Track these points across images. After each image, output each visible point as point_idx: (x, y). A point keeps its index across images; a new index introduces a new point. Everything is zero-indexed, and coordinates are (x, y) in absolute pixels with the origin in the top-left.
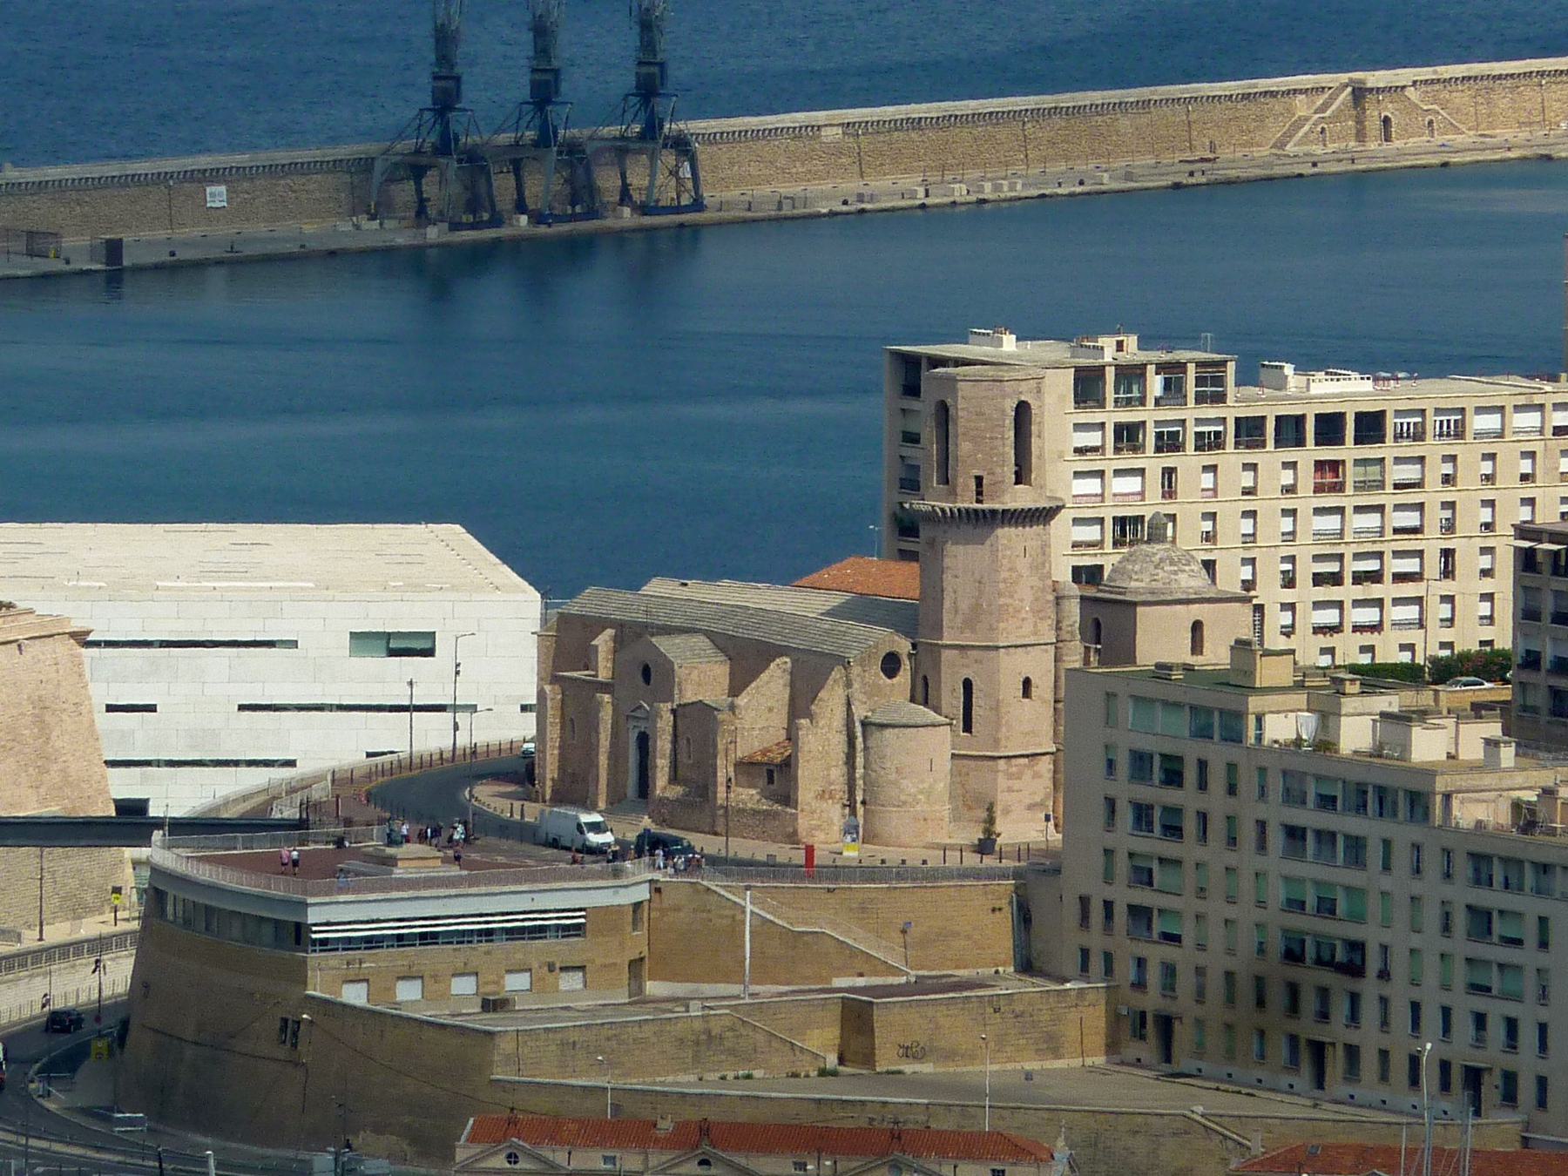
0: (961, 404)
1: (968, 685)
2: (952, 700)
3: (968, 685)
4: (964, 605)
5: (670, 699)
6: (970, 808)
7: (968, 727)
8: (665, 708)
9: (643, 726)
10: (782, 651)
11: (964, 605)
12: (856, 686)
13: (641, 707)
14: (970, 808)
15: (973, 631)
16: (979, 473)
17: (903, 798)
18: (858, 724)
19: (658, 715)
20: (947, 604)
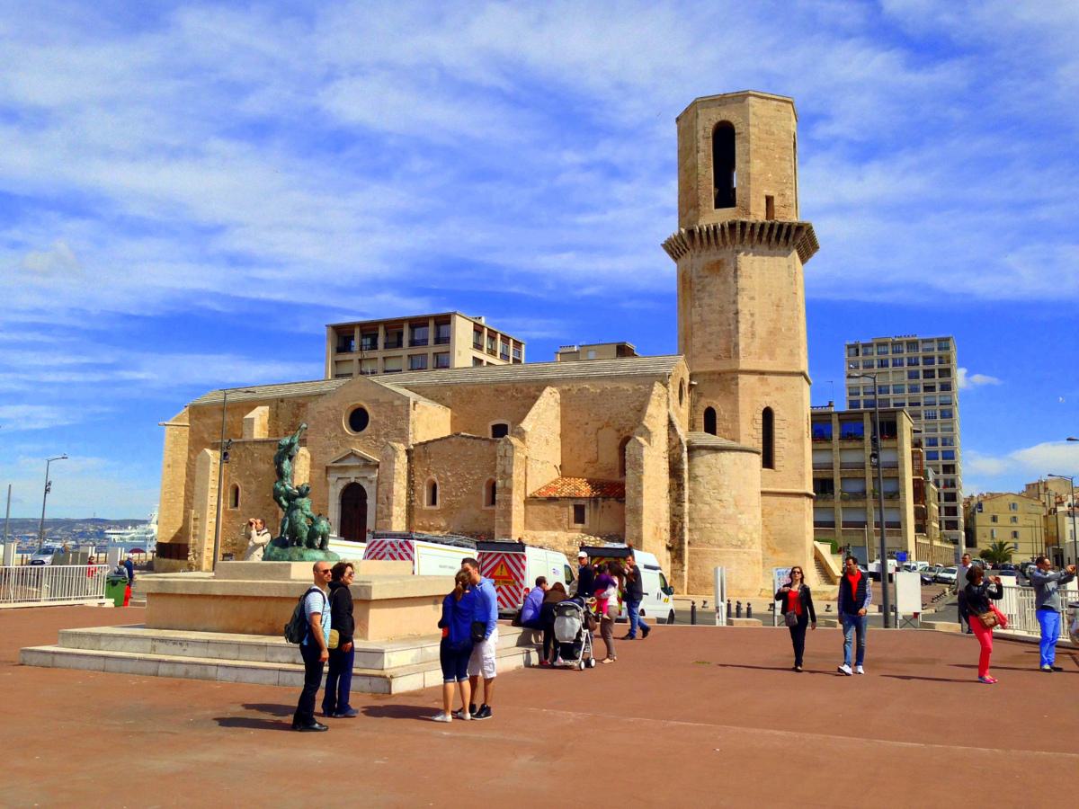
0: (753, 120)
1: (768, 415)
2: (751, 434)
3: (768, 415)
4: (761, 330)
5: (403, 435)
6: (775, 552)
7: (768, 462)
8: (401, 447)
9: (352, 477)
10: (550, 382)
11: (761, 330)
12: (671, 407)
13: (353, 454)
14: (775, 552)
15: (772, 355)
16: (771, 193)
17: (741, 536)
18: (686, 449)
19: (390, 459)
20: (743, 327)
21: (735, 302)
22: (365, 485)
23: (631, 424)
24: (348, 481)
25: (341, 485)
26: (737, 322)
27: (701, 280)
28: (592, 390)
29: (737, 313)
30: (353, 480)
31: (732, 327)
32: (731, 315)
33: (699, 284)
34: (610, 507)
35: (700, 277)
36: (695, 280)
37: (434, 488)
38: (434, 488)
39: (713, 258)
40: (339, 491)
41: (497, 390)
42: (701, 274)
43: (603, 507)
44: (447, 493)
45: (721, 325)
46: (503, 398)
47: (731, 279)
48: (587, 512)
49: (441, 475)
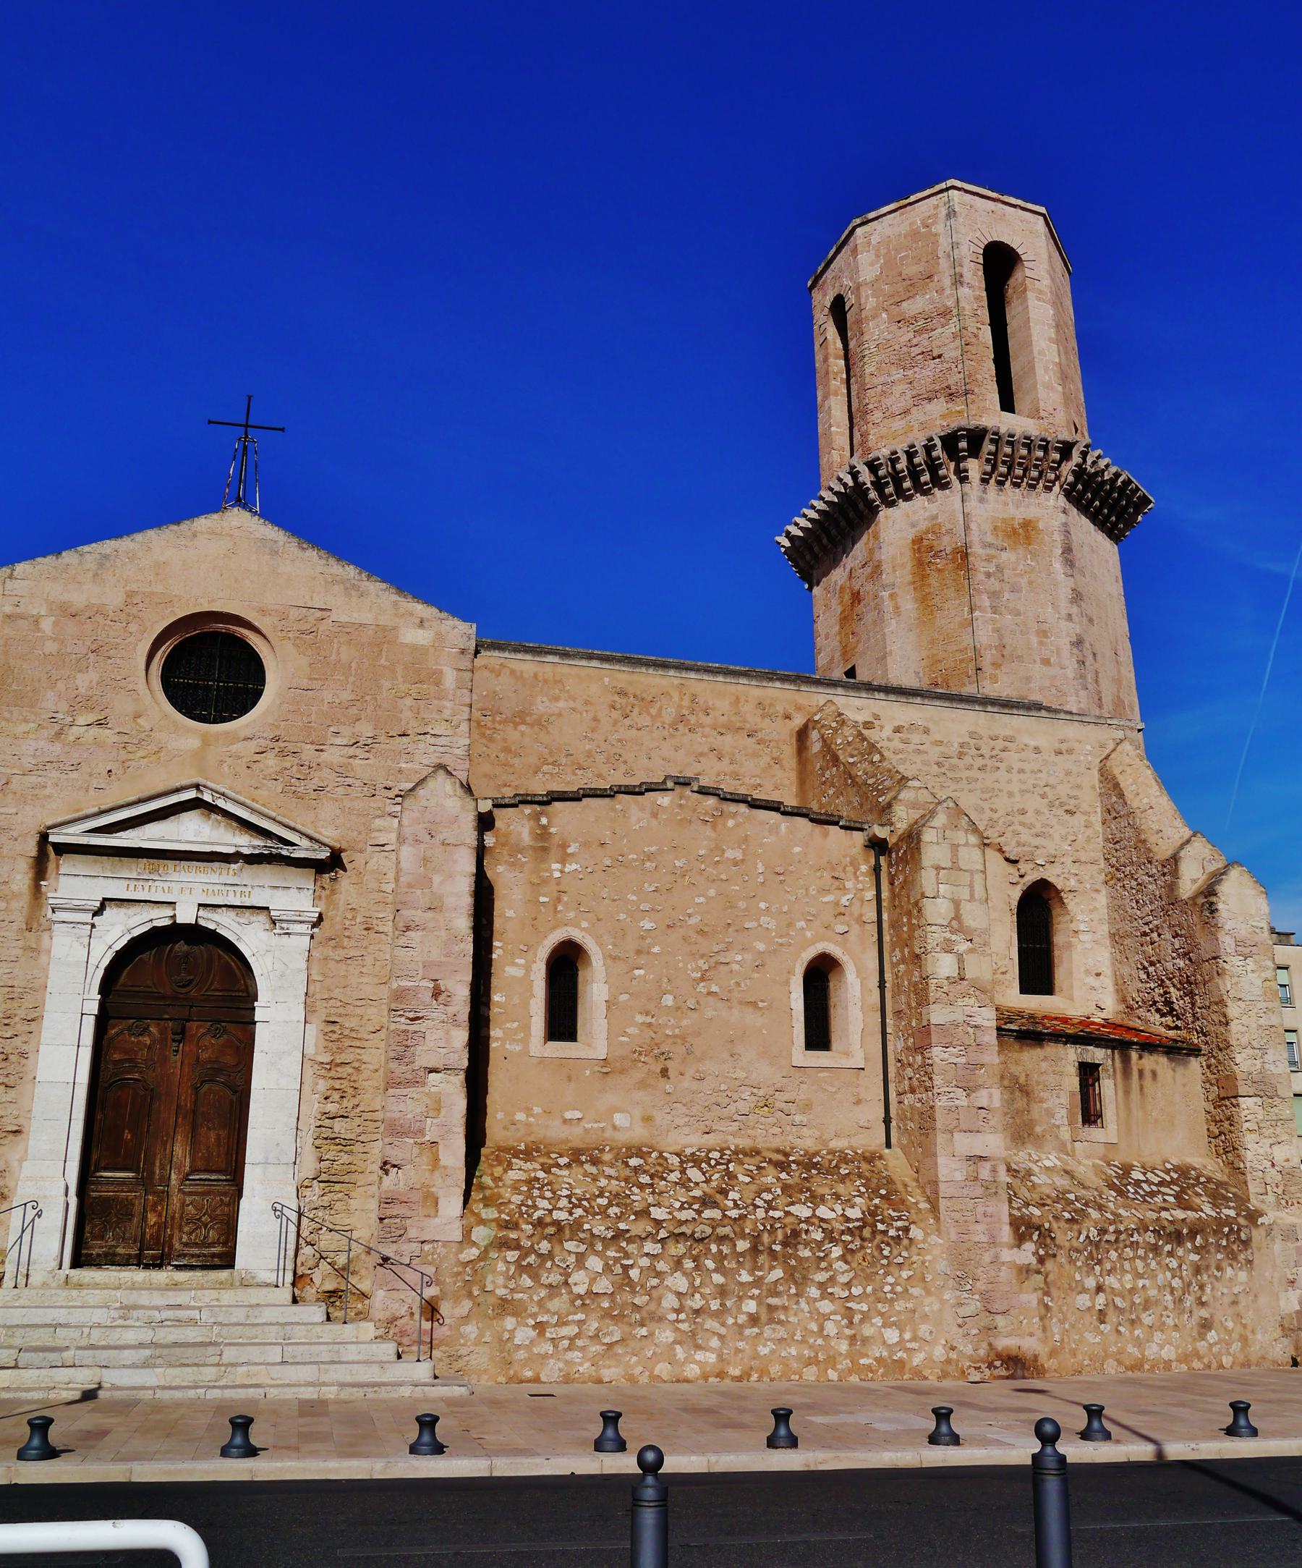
9: (186, 897)
23: (1051, 847)
24: (161, 918)
25: (118, 930)
27: (988, 551)
30: (186, 915)
33: (989, 559)
34: (1154, 1074)
35: (990, 545)
36: (977, 549)
37: (565, 966)
39: (1019, 514)
40: (102, 956)
41: (622, 693)
42: (990, 538)
43: (1141, 1073)
45: (1046, 662)
46: (644, 720)
47: (1058, 566)
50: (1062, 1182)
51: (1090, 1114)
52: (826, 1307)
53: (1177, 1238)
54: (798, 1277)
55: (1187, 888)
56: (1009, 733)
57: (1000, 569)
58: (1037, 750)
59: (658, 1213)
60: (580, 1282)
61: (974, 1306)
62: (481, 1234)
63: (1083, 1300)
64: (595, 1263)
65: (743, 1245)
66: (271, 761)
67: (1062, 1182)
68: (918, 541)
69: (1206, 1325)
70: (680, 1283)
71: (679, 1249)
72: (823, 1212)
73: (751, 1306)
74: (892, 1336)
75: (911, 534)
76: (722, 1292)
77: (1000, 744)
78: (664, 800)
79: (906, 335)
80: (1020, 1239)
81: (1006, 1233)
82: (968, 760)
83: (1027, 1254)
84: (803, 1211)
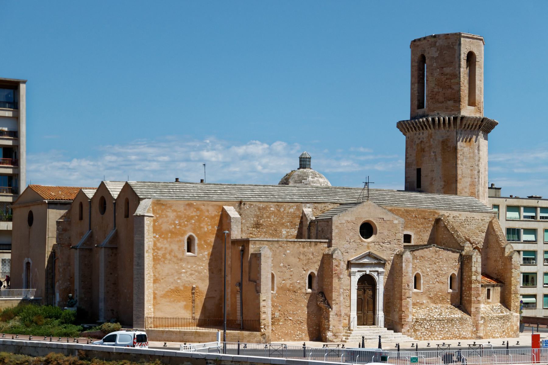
9: (368, 270)
21: (478, 165)
22: (375, 275)
25: (358, 276)
26: (479, 177)
28: (460, 218)
29: (479, 172)
30: (368, 273)
31: (476, 180)
32: (476, 172)
38: (417, 279)
44: (427, 282)
47: (476, 151)
48: (491, 292)
49: (424, 271)
50: (485, 310)
51: (488, 297)
52: (456, 329)
53: (501, 318)
54: (453, 325)
55: (506, 254)
56: (473, 216)
57: (463, 153)
58: (478, 220)
59: (435, 317)
60: (426, 326)
61: (475, 329)
62: (414, 320)
63: (488, 328)
64: (428, 324)
65: (446, 321)
66: (377, 246)
67: (485, 310)
68: (443, 142)
69: (503, 332)
70: (438, 327)
71: (438, 322)
72: (456, 316)
73: (447, 330)
74: (464, 333)
75: (441, 139)
76: (443, 328)
77: (472, 219)
78: (431, 249)
79: (444, 78)
80: (482, 320)
81: (480, 319)
82: (466, 223)
83: (482, 322)
84: (453, 316)
